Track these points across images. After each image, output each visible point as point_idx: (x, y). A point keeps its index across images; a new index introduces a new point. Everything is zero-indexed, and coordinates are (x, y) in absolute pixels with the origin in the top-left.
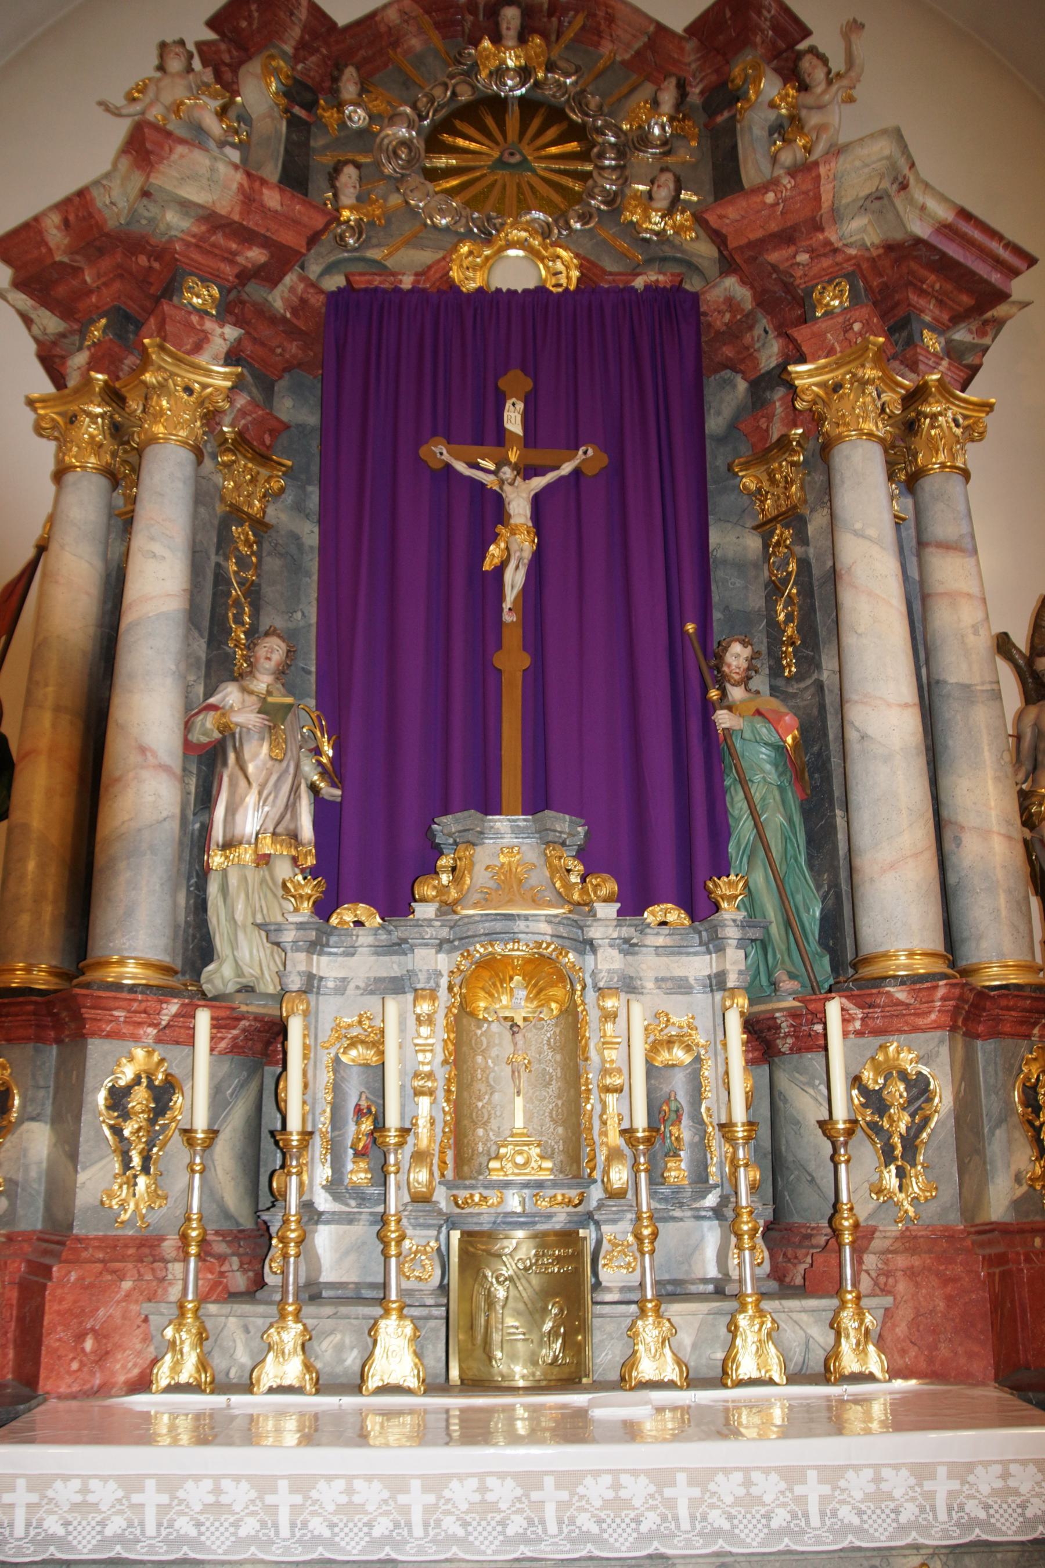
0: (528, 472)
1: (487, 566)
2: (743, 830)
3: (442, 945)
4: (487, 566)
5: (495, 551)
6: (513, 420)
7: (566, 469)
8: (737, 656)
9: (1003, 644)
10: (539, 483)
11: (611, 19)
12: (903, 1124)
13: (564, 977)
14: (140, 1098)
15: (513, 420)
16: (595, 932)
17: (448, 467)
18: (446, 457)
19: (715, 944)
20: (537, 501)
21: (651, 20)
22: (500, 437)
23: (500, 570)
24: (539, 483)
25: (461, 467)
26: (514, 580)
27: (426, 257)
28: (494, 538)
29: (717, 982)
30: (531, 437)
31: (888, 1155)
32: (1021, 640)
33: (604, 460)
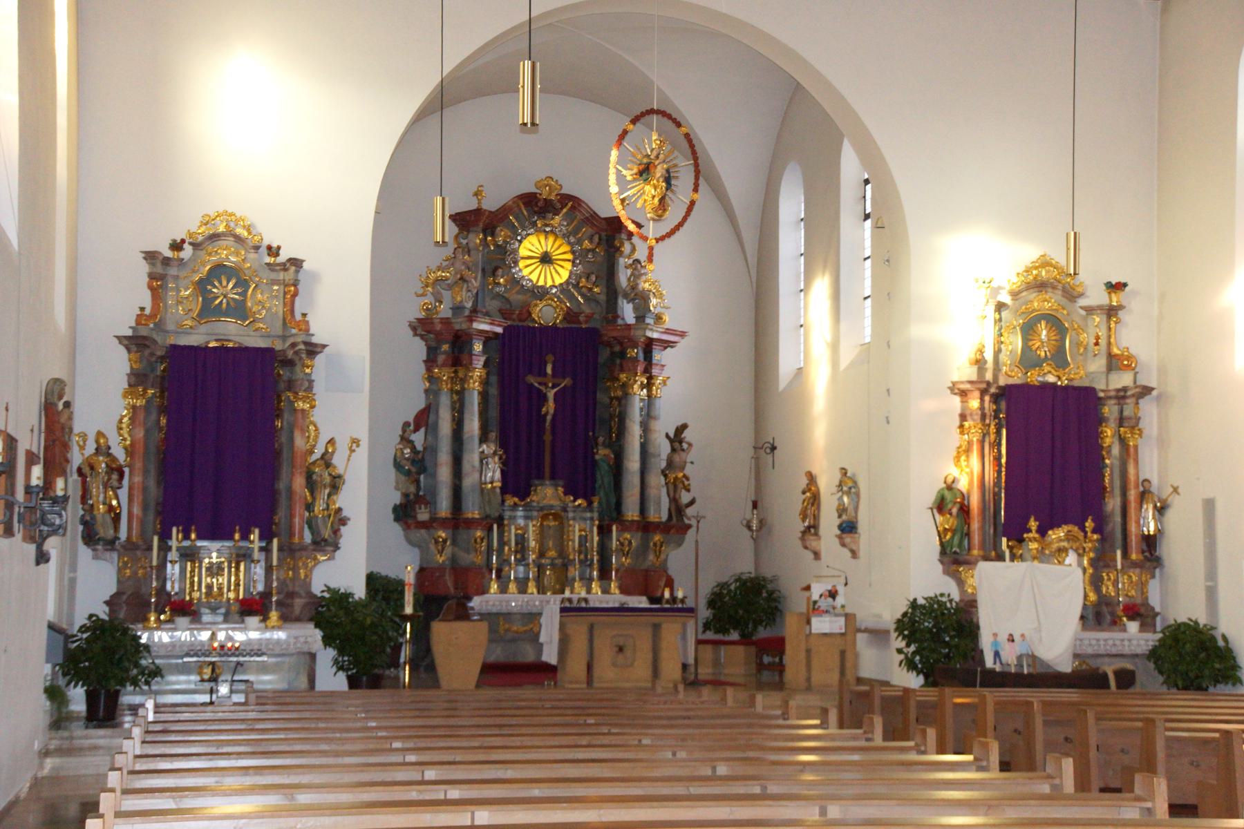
0: (553, 387)
1: (543, 413)
2: (599, 482)
3: (538, 511)
4: (543, 413)
5: (544, 409)
6: (549, 370)
7: (562, 385)
8: (601, 439)
9: (667, 436)
10: (555, 390)
11: (580, 205)
12: (627, 549)
13: (561, 517)
14: (478, 540)
15: (549, 370)
16: (568, 509)
17: (532, 385)
18: (532, 381)
19: (591, 511)
20: (555, 394)
21: (592, 210)
22: (545, 374)
23: (547, 413)
24: (555, 390)
25: (536, 385)
26: (549, 418)
27: (520, 297)
28: (544, 405)
29: (592, 519)
30: (554, 375)
31: (624, 554)
32: (672, 435)
33: (571, 382)
